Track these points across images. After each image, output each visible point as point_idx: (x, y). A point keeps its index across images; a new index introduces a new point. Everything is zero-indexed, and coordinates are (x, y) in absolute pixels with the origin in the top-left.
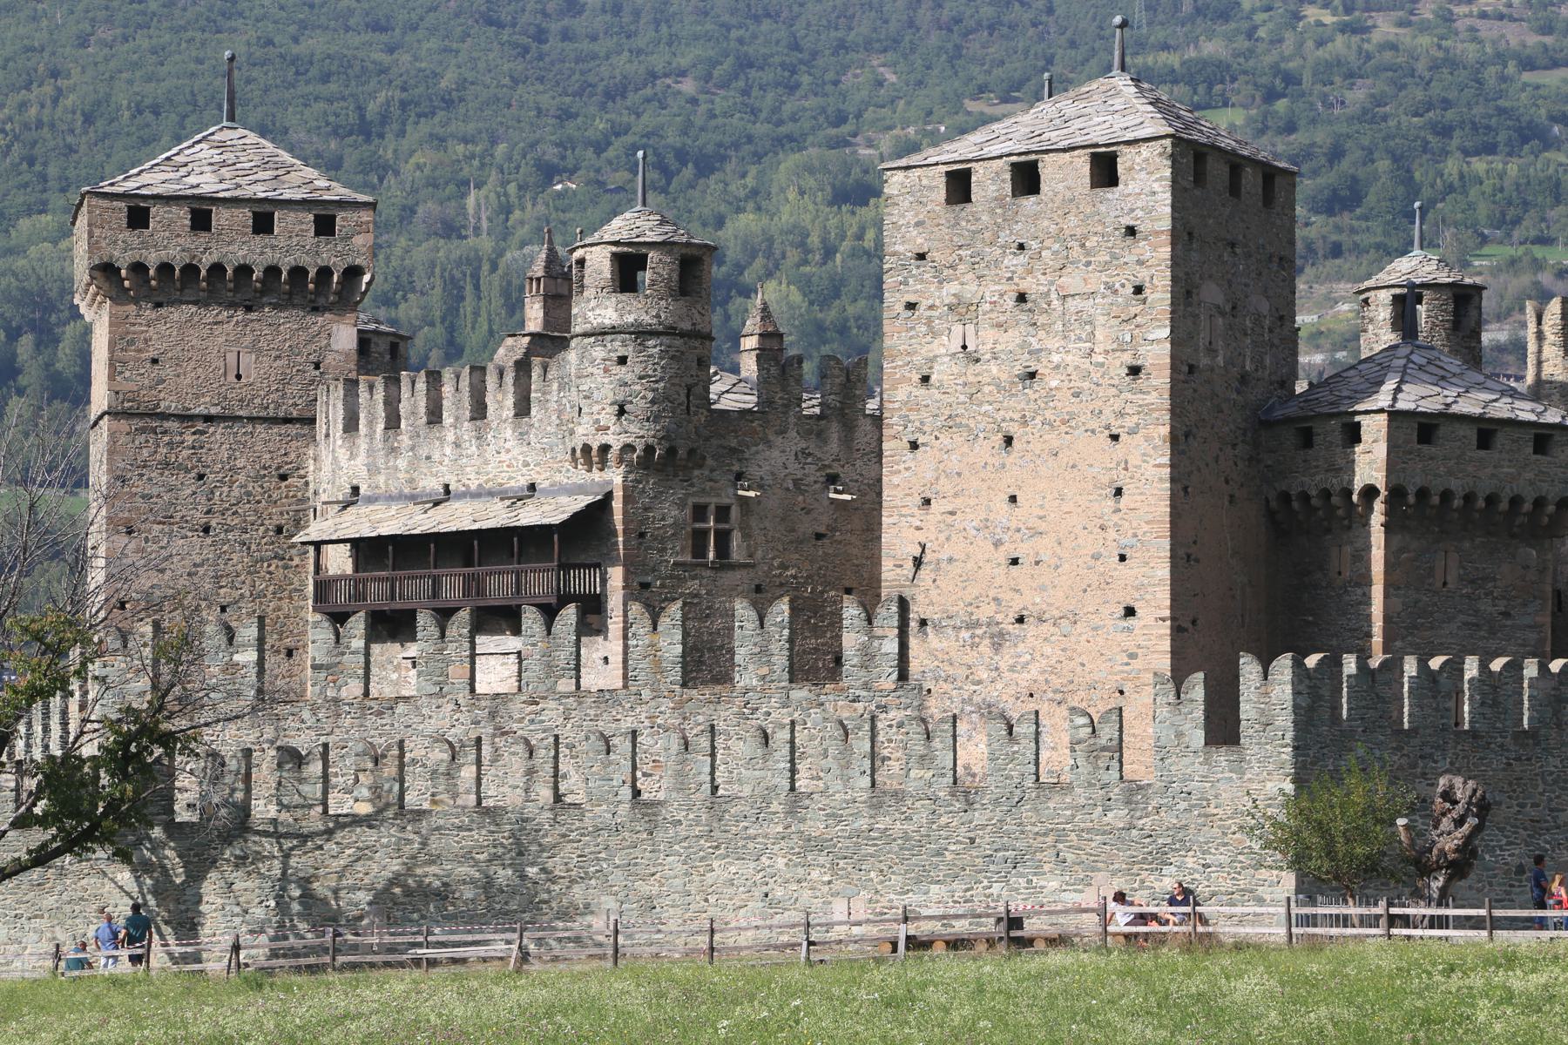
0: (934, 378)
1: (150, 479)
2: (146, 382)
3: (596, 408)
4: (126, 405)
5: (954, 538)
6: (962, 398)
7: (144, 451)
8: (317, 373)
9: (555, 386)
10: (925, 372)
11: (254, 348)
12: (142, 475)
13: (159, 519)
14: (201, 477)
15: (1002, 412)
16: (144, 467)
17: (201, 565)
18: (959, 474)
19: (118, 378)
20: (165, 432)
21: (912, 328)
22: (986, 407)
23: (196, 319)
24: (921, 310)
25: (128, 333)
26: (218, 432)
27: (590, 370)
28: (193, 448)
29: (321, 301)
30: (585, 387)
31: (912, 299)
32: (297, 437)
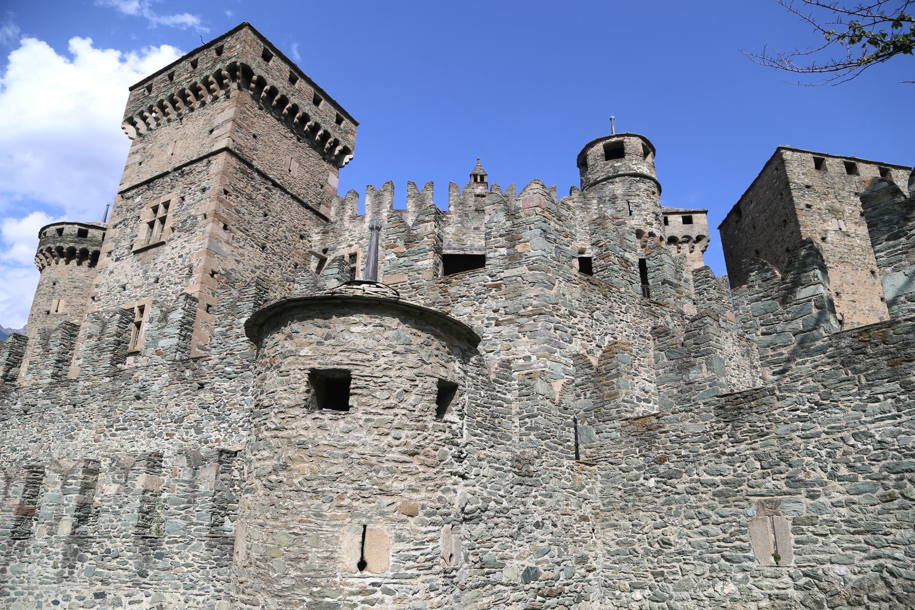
0: (829, 239)
1: (241, 202)
2: (249, 145)
3: (643, 212)
4: (237, 151)
5: (858, 313)
6: (845, 250)
7: (241, 183)
8: (322, 191)
9: (595, 201)
10: (824, 236)
11: (298, 161)
12: (238, 197)
13: (241, 228)
14: (266, 215)
15: (867, 260)
16: (239, 192)
17: (258, 268)
18: (853, 284)
19: (236, 133)
20: (252, 179)
21: (812, 216)
22: (857, 257)
23: (277, 128)
24: (814, 208)
25: (245, 113)
26: (277, 193)
27: (637, 193)
28: (265, 196)
29: (327, 157)
30: (634, 201)
31: (809, 203)
32: (310, 219)
